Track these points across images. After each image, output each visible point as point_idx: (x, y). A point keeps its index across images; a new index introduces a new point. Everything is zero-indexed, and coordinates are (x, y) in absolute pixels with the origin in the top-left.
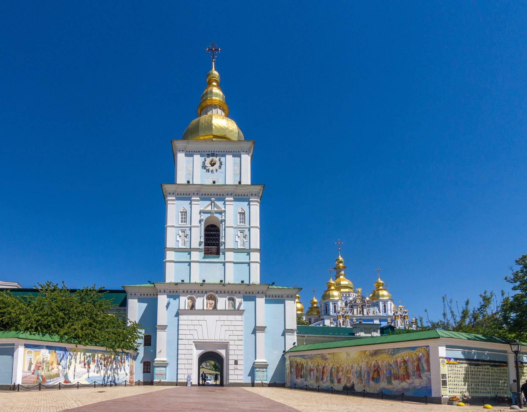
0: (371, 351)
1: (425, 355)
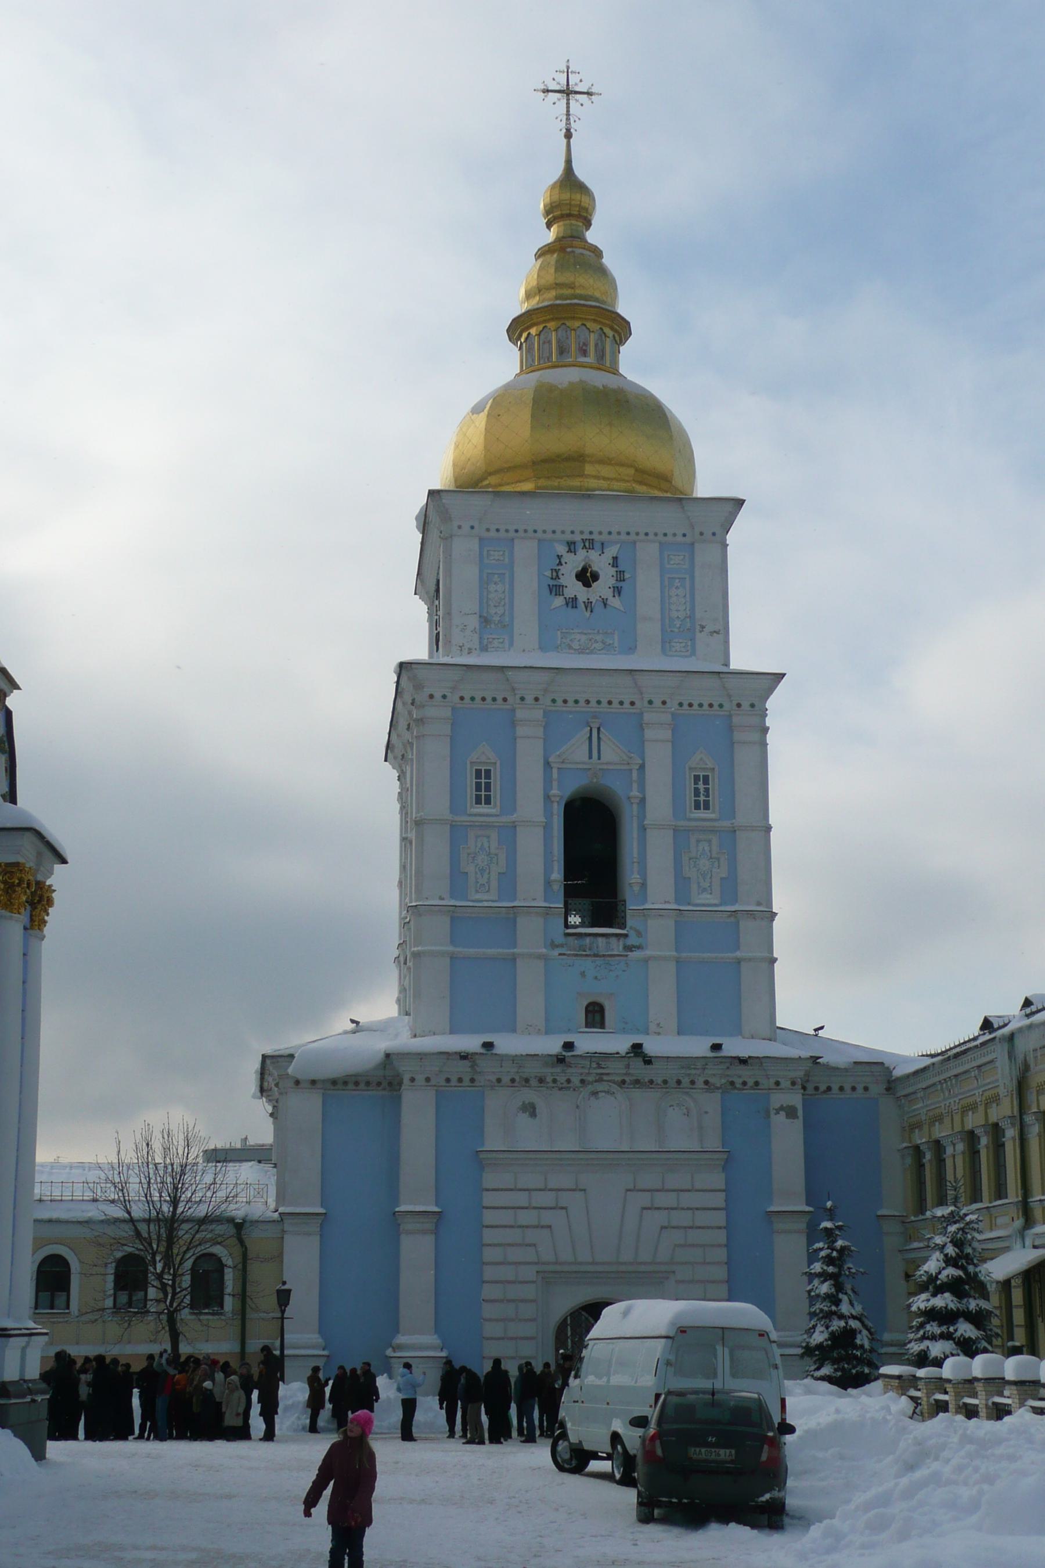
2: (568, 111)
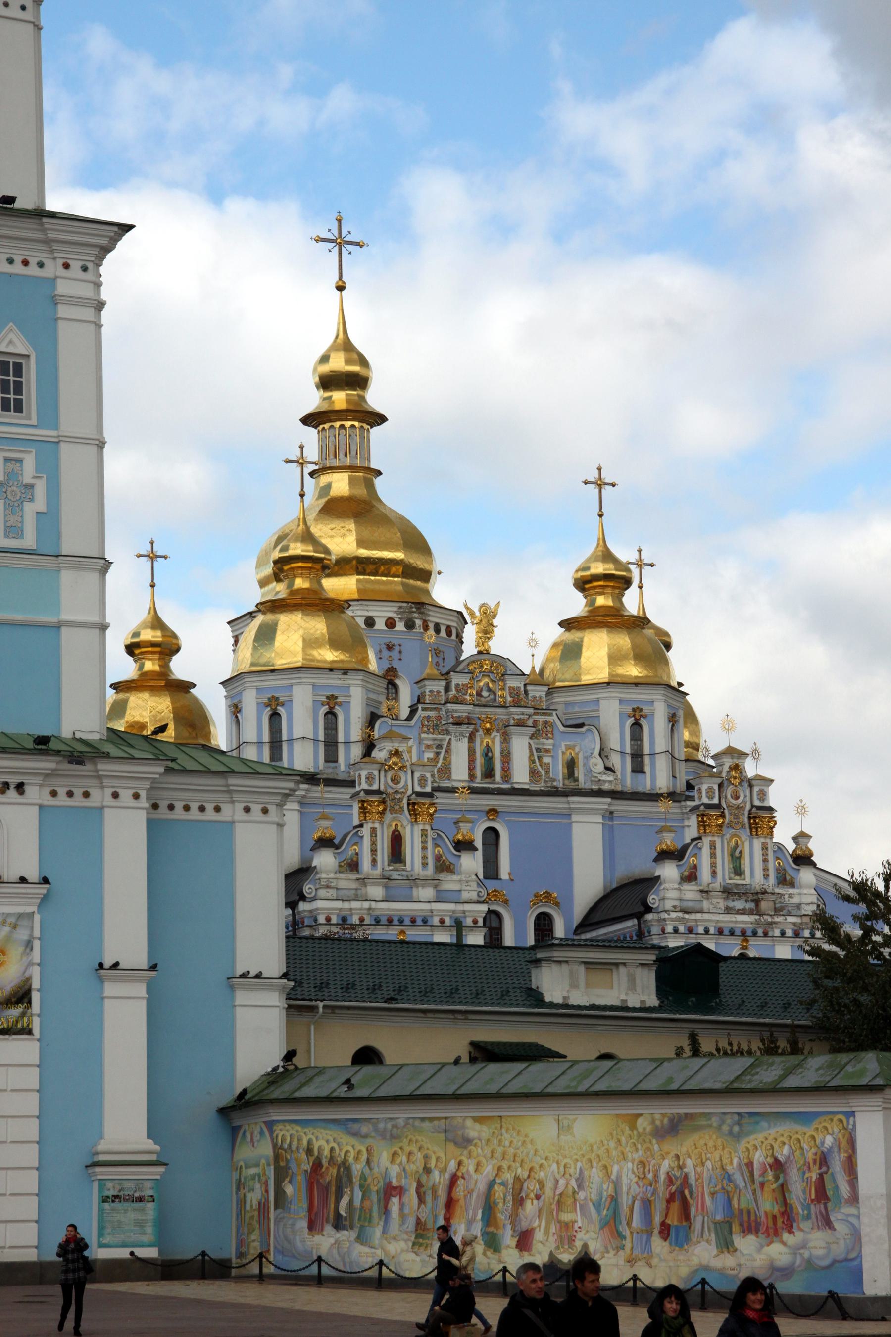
1: (841, 1146)
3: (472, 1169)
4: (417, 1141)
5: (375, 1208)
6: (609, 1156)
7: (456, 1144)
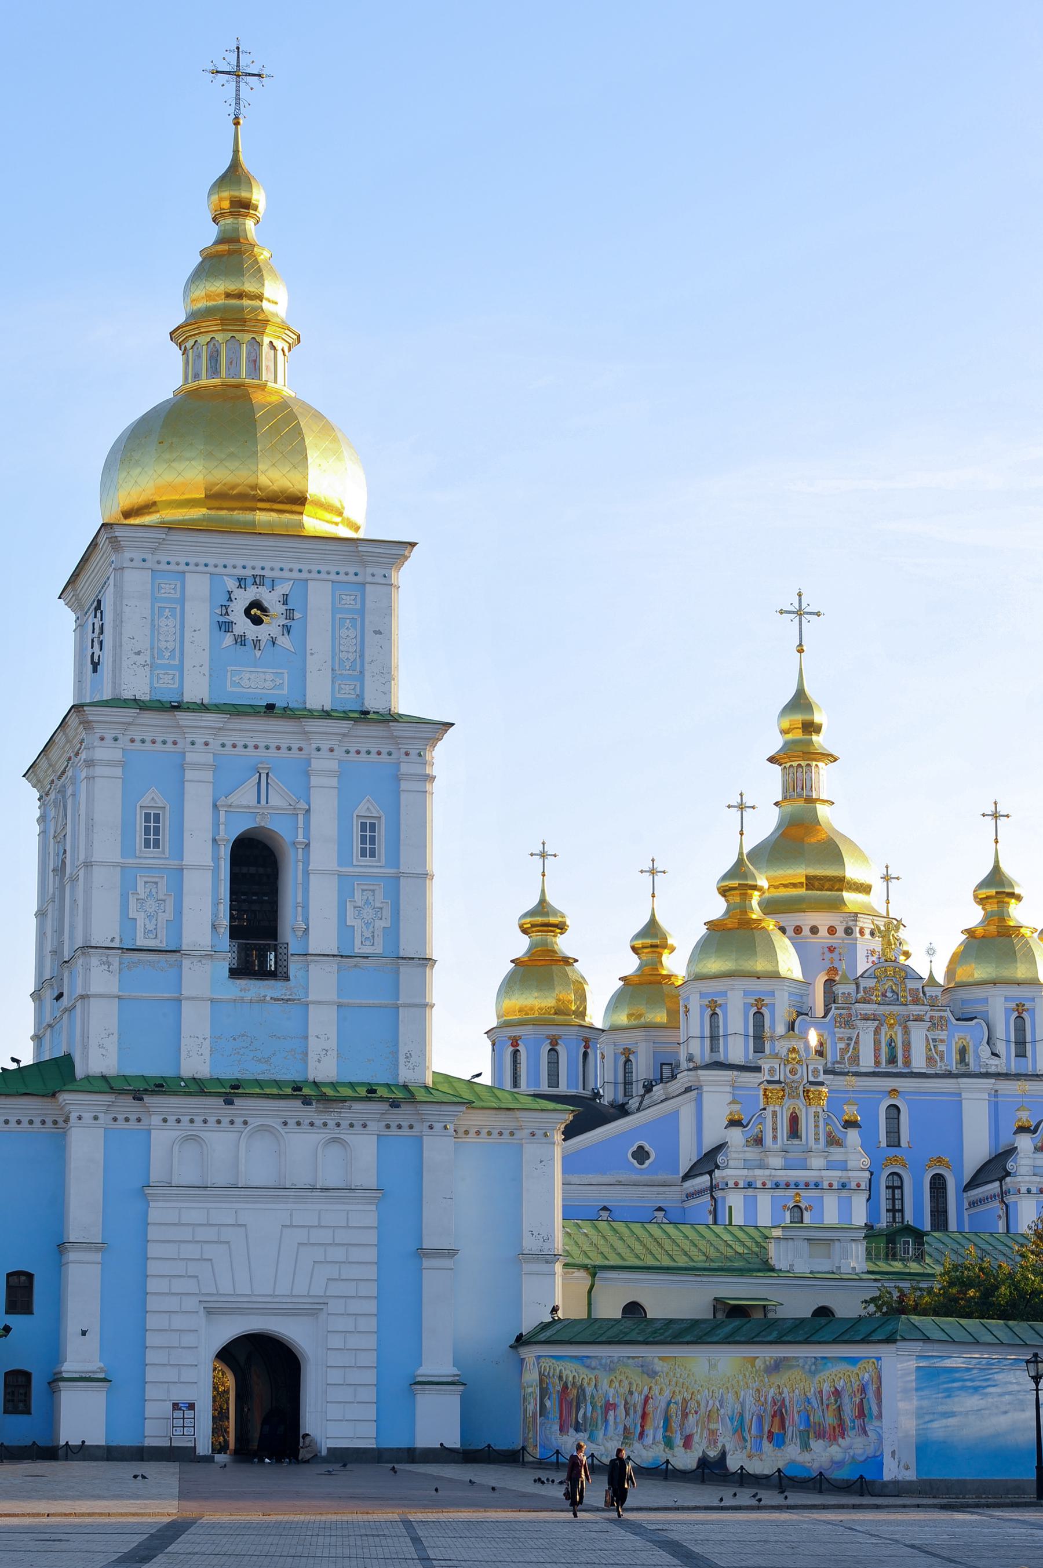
0: (767, 1358)
2: (238, 95)
3: (657, 1392)
4: (625, 1373)
5: (600, 1417)
6: (738, 1386)
7: (648, 1375)
